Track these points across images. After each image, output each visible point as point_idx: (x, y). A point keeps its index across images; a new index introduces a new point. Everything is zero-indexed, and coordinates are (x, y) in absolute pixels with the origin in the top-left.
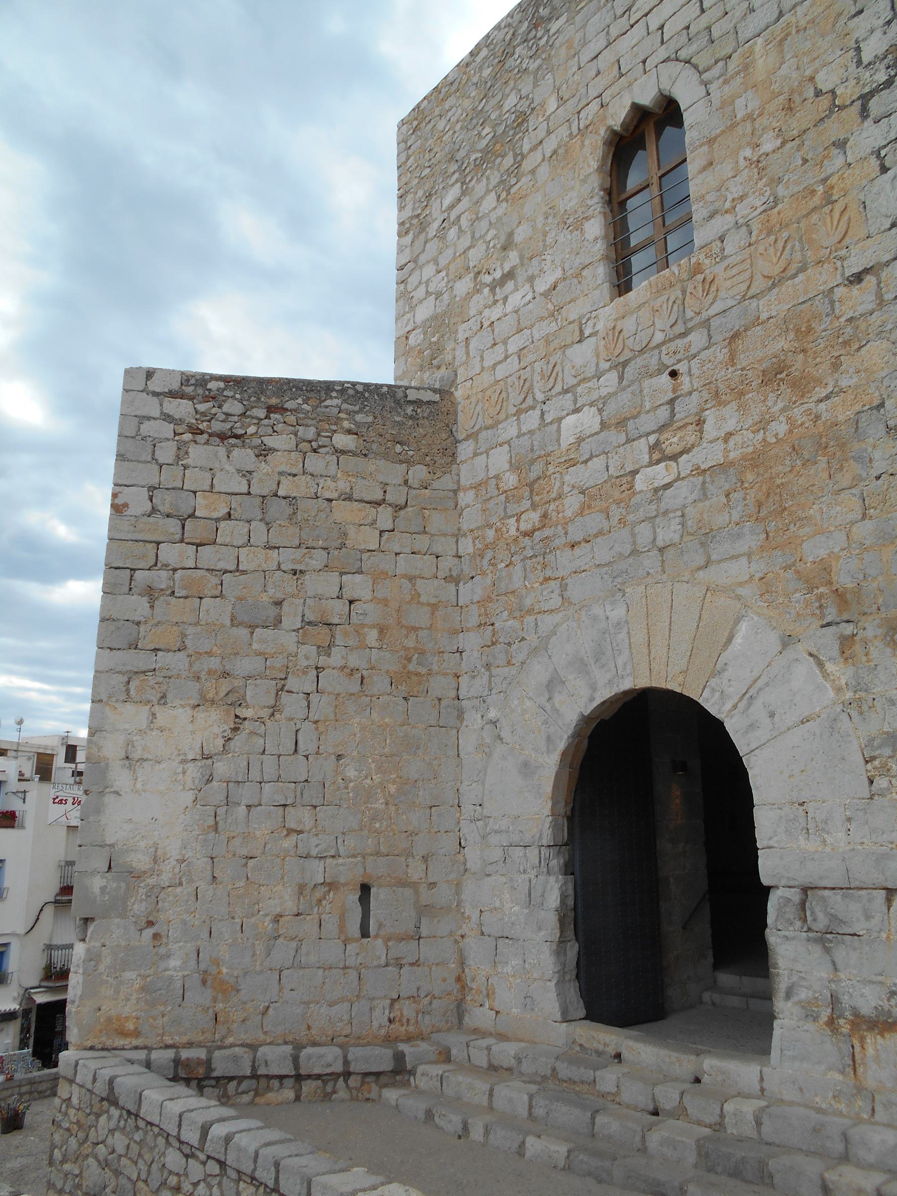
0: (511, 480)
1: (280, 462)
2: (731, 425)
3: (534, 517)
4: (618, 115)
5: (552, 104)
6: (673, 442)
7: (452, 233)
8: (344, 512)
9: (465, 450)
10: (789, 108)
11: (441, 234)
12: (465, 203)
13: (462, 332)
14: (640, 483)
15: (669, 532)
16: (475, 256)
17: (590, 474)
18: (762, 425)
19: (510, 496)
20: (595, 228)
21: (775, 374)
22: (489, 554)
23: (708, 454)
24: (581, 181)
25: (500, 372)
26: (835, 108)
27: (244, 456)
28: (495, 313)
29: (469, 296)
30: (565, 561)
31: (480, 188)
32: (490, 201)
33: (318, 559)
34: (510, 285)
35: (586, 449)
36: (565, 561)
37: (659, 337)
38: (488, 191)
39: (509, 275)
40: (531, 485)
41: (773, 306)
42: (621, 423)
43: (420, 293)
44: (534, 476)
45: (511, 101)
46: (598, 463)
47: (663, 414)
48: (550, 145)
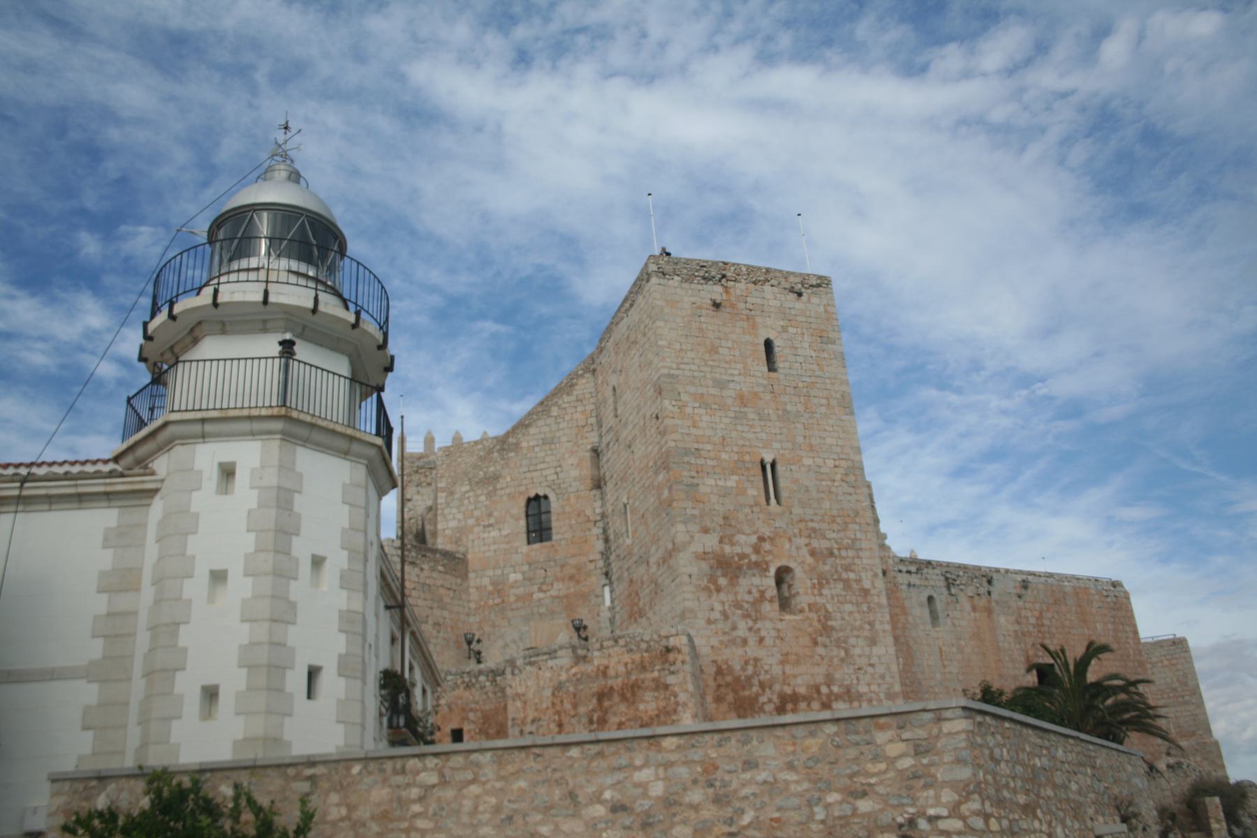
0: (490, 588)
1: (426, 573)
3: (498, 601)
4: (532, 495)
5: (508, 479)
6: (544, 588)
7: (466, 502)
8: (442, 591)
9: (472, 575)
10: (579, 515)
11: (461, 500)
12: (471, 494)
13: (471, 537)
14: (535, 596)
15: (542, 610)
16: (477, 513)
17: (520, 591)
18: (568, 588)
19: (490, 593)
20: (523, 523)
21: (571, 578)
23: (554, 592)
24: (519, 508)
25: (487, 554)
26: (589, 521)
27: (417, 570)
28: (486, 535)
29: (473, 526)
30: (510, 614)
31: (479, 492)
32: (483, 498)
33: (435, 605)
36: (510, 614)
39: (489, 525)
40: (499, 591)
41: (573, 561)
42: (530, 579)
43: (450, 517)
44: (499, 587)
48: (508, 491)
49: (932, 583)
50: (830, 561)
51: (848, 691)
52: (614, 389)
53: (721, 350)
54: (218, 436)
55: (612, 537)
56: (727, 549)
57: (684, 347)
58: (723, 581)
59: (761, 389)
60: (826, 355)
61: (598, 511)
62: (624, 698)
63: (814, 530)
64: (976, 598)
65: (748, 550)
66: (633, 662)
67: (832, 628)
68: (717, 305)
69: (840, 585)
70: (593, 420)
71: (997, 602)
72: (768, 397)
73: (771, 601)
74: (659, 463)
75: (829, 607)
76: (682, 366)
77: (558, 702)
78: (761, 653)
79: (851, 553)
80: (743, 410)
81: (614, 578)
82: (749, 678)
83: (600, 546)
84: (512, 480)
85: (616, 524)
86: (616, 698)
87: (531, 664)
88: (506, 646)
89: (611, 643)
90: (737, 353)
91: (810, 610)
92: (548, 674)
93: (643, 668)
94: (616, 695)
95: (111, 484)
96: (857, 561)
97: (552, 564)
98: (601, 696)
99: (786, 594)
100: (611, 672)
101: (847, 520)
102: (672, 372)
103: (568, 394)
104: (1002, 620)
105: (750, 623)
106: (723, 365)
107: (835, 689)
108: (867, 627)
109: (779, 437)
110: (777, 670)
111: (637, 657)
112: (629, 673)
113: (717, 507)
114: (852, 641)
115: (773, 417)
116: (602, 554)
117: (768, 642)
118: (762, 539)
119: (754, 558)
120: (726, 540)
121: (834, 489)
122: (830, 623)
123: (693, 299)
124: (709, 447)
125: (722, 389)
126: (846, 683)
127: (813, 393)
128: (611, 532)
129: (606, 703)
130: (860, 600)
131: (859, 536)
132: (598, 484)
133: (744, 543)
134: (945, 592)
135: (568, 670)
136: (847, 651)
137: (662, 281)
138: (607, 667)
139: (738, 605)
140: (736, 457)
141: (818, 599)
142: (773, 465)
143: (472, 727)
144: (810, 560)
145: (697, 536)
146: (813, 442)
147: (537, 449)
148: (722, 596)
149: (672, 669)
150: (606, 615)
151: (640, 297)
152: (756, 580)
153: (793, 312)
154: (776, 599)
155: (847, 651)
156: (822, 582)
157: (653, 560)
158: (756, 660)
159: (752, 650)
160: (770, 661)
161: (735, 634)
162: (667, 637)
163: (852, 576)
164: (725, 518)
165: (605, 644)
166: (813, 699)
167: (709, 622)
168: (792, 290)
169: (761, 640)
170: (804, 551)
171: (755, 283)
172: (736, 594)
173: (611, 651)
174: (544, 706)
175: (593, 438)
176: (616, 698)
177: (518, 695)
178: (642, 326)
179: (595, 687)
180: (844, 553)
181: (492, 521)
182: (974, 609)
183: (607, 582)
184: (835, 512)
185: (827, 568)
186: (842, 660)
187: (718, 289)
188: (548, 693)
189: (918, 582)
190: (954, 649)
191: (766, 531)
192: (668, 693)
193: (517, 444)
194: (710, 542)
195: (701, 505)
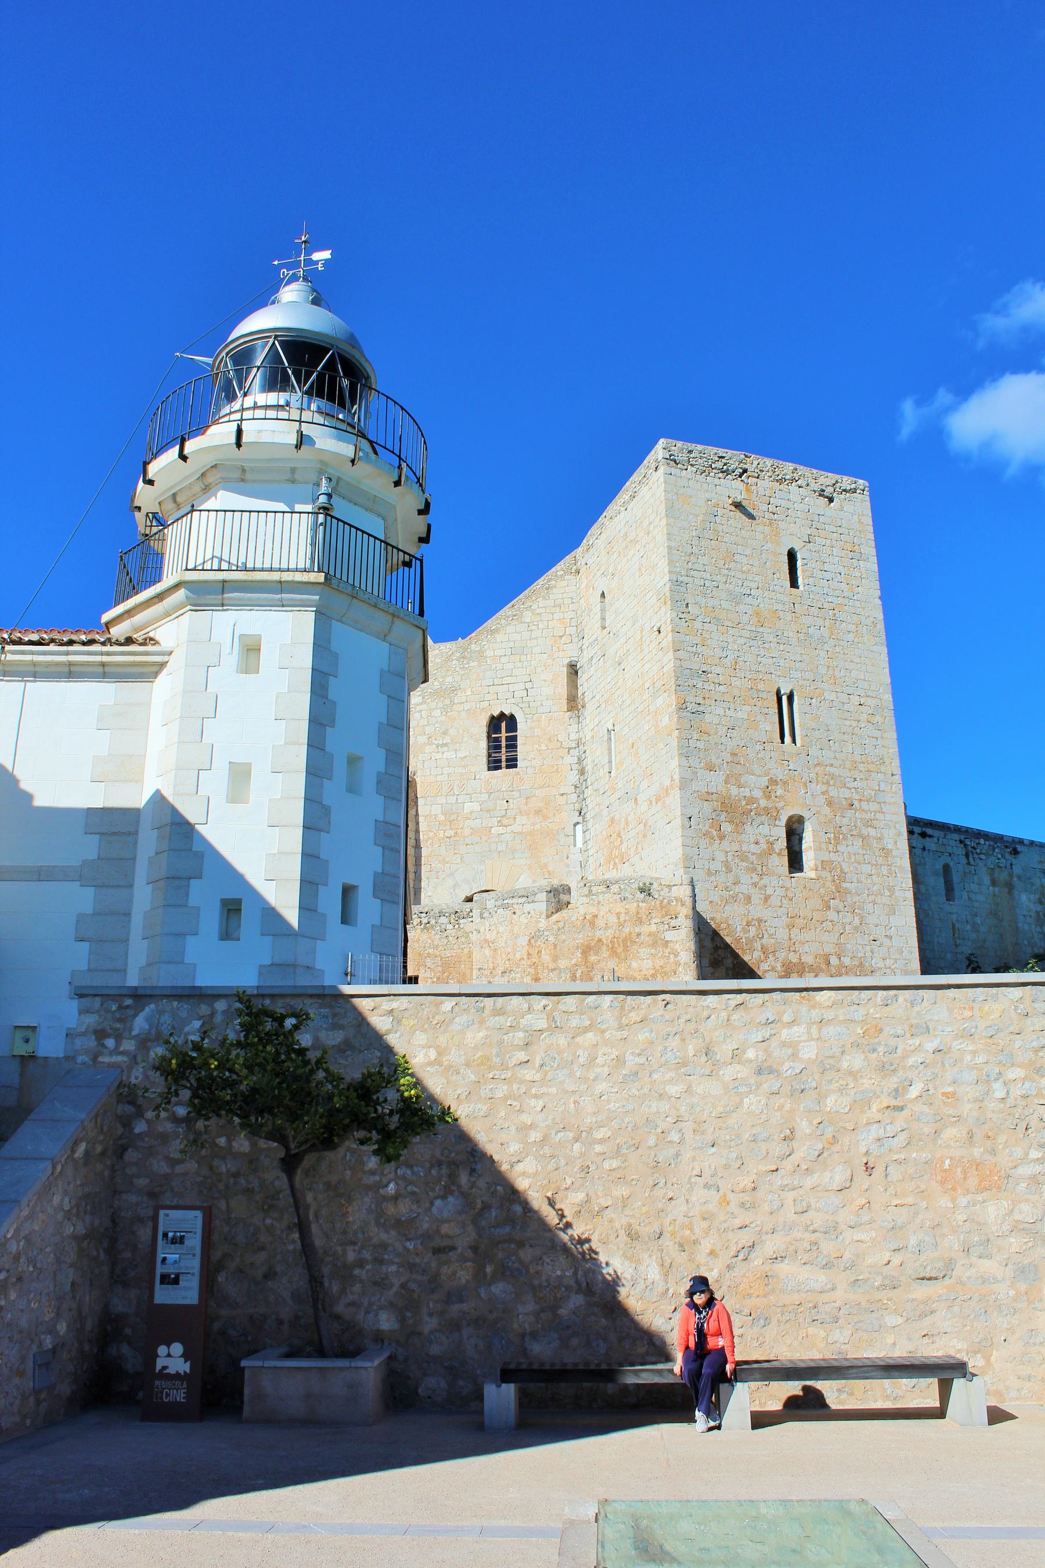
0: (442, 818)
2: (524, 822)
3: (452, 833)
6: (505, 821)
9: (420, 802)
12: (424, 707)
15: (502, 847)
16: (429, 730)
18: (533, 824)
20: (483, 744)
21: (538, 812)
22: (430, 841)
23: (516, 828)
25: (439, 778)
31: (433, 705)
34: (446, 749)
35: (474, 815)
37: (504, 789)
38: (436, 708)
39: (446, 745)
45: (449, 679)
46: (478, 821)
47: (503, 812)
48: (467, 706)
49: (949, 849)
50: (849, 813)
51: (861, 965)
52: (603, 595)
53: (737, 557)
54: (240, 605)
55: (589, 768)
56: (734, 791)
57: (695, 550)
58: (727, 828)
59: (780, 607)
60: (858, 574)
61: (573, 736)
62: (614, 952)
63: (833, 776)
64: (997, 870)
65: (758, 794)
66: (627, 913)
67: (847, 892)
68: (738, 505)
69: (858, 842)
70: (572, 630)
71: (1019, 878)
72: (789, 616)
73: (779, 854)
74: (658, 684)
75: (845, 866)
76: (692, 573)
77: (534, 952)
78: (766, 914)
79: (874, 806)
80: (761, 630)
81: (588, 816)
82: (750, 941)
83: (573, 777)
84: (473, 693)
85: (595, 754)
86: (605, 953)
87: (505, 907)
88: (455, 886)
89: (603, 888)
90: (757, 564)
91: (824, 868)
92: (524, 920)
93: (640, 921)
94: (604, 948)
95: (108, 654)
96: (879, 816)
97: (516, 794)
98: (586, 950)
99: (797, 848)
100: (600, 923)
101: (871, 767)
102: (680, 579)
103: (544, 598)
104: (1024, 898)
105: (756, 878)
106: (738, 575)
107: (847, 961)
108: (887, 893)
109: (798, 665)
110: (782, 934)
111: (632, 907)
112: (621, 925)
113: (723, 740)
114: (869, 907)
115: (794, 641)
116: (576, 787)
117: (775, 901)
118: (773, 782)
119: (763, 803)
120: (733, 780)
121: (857, 731)
122: (844, 885)
123: (708, 495)
124: (718, 670)
125: (737, 604)
126: (860, 955)
127: (841, 616)
128: (588, 764)
129: (593, 958)
130: (880, 861)
131: (883, 786)
132: (573, 702)
133: (754, 785)
134: (964, 860)
135: (548, 917)
136: (862, 918)
137: (673, 471)
138: (596, 916)
139: (743, 856)
140: (749, 685)
141: (833, 857)
142: (790, 697)
143: (428, 974)
144: (827, 810)
145: (700, 772)
146: (836, 673)
147: (504, 660)
148: (725, 843)
149: (673, 923)
150: (576, 857)
151: (645, 489)
152: (765, 829)
153: (822, 519)
154: (786, 853)
155: (862, 918)
156: (836, 837)
157: (642, 798)
158: (760, 921)
159: (756, 910)
160: (776, 922)
161: (737, 889)
162: (670, 887)
163: (872, 832)
164: (734, 755)
165: (594, 889)
166: (822, 970)
167: (709, 873)
168: (821, 493)
169: (767, 898)
170: (822, 799)
171: (780, 481)
172: (741, 843)
173: (601, 898)
174: (518, 956)
175: (571, 653)
176: (605, 953)
177: (486, 941)
178: (646, 522)
179: (580, 939)
180: (864, 804)
181: (447, 740)
182: (994, 883)
183: (580, 819)
184: (858, 758)
185: (845, 821)
186: (856, 929)
187: (738, 483)
188: (523, 941)
189: (933, 847)
190: (968, 927)
191: (780, 774)
192: (667, 951)
193: (481, 653)
194: (716, 781)
195: (705, 737)
